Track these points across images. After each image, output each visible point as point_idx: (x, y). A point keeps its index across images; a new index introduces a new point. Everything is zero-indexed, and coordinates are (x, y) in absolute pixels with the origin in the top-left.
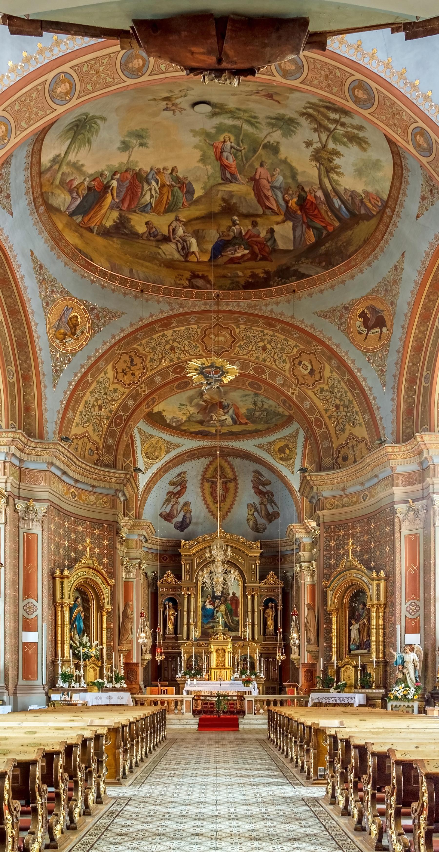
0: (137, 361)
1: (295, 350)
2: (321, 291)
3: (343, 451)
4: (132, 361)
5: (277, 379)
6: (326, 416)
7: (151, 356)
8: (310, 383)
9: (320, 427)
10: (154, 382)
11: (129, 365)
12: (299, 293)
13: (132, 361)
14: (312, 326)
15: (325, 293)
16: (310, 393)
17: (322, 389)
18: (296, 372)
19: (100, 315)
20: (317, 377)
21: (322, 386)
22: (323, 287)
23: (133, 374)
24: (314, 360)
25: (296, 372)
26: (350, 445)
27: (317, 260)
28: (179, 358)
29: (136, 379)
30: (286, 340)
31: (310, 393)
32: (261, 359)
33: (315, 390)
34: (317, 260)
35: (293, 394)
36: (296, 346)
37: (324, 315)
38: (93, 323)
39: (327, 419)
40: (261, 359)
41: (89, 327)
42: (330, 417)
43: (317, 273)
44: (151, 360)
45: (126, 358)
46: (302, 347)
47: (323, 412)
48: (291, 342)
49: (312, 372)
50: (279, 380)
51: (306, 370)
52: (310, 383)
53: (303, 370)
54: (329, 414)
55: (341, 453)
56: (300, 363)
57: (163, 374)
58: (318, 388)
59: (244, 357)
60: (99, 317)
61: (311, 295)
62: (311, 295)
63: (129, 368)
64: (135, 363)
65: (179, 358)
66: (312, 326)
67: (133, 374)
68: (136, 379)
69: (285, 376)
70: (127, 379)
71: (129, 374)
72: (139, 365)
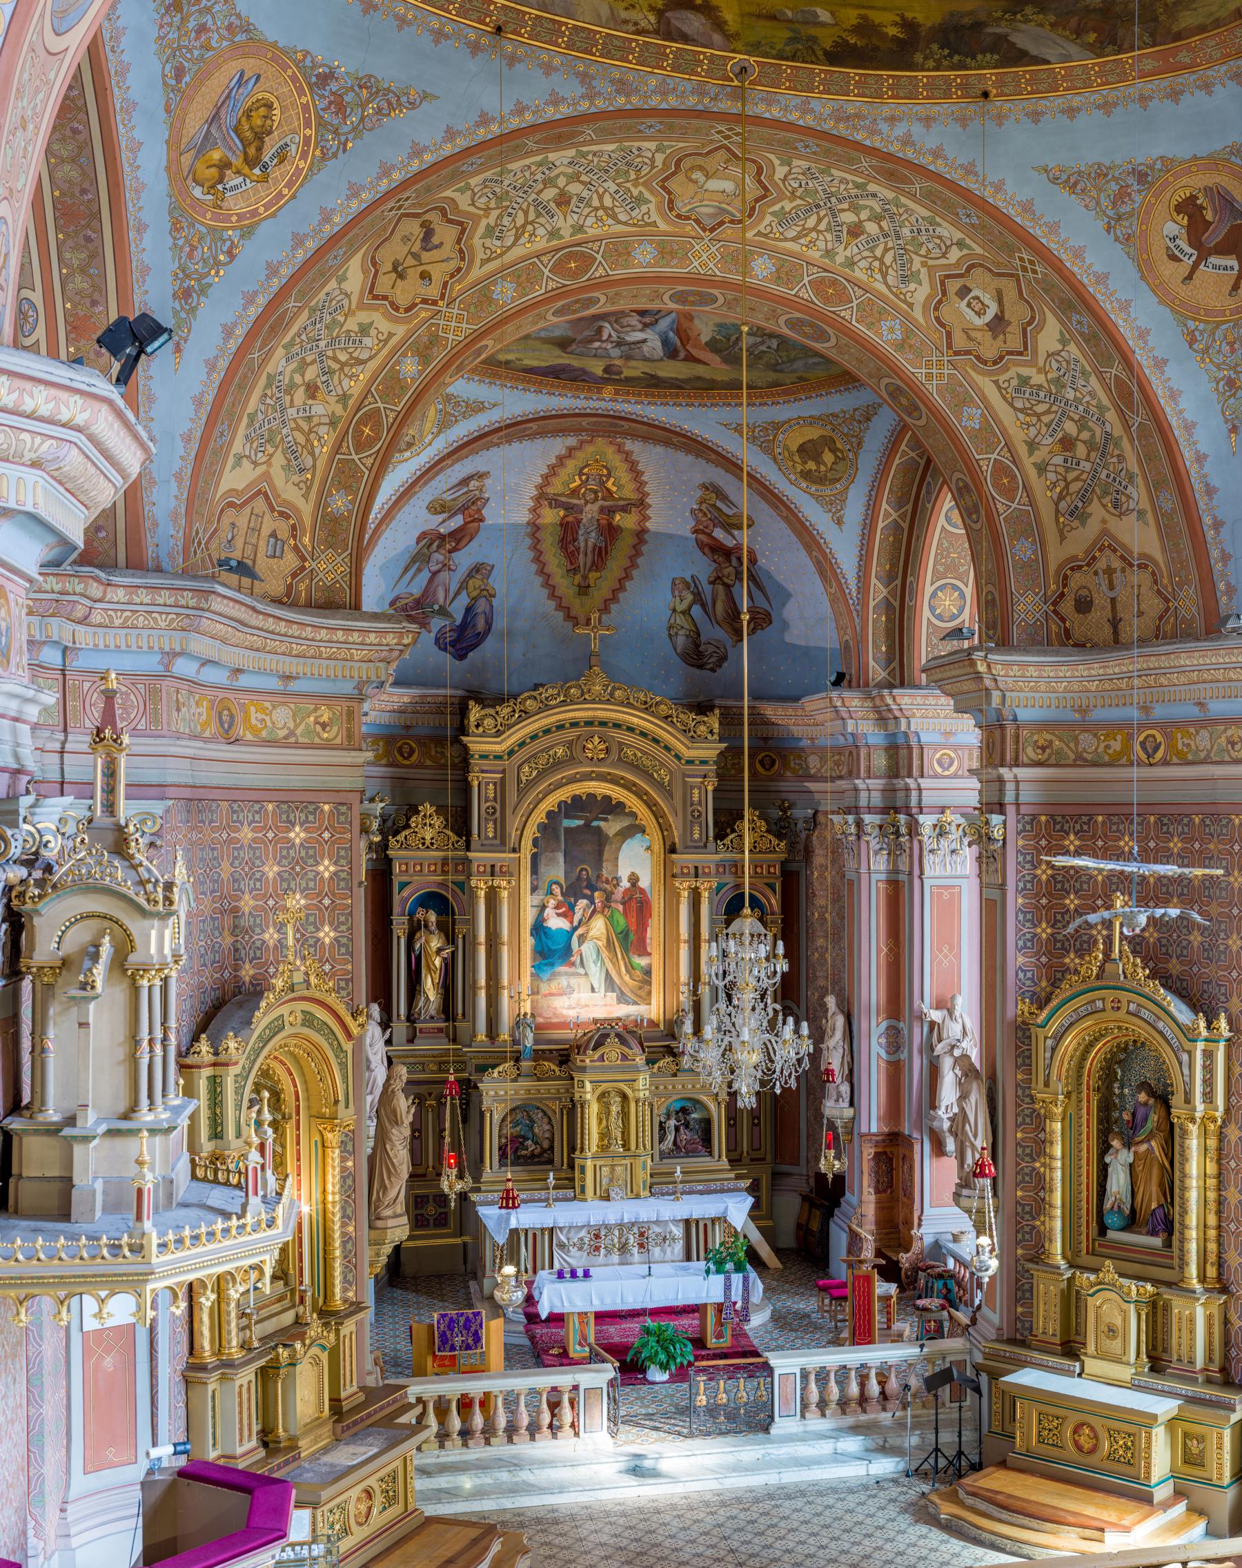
0: (445, 234)
1: (955, 254)
2: (1071, 112)
3: (1077, 580)
4: (428, 233)
5: (885, 325)
6: (1028, 462)
7: (492, 220)
8: (989, 352)
9: (1010, 493)
10: (490, 300)
11: (416, 248)
12: (998, 104)
13: (428, 233)
14: (1027, 207)
15: (1082, 119)
16: (986, 384)
17: (1024, 381)
18: (946, 313)
19: (348, 98)
20: (1014, 342)
21: (1025, 371)
22: (1076, 101)
23: (425, 276)
24: (1010, 295)
25: (946, 313)
26: (1101, 564)
27: (1074, 21)
28: (579, 228)
29: (433, 291)
30: (932, 223)
31: (986, 384)
32: (840, 259)
33: (1002, 378)
34: (1074, 21)
35: (929, 376)
36: (960, 244)
37: (1071, 182)
38: (321, 123)
39: (1032, 473)
40: (840, 259)
41: (307, 140)
42: (1042, 468)
43: (1068, 58)
44: (490, 232)
45: (413, 228)
46: (979, 251)
47: (1022, 450)
48: (947, 231)
49: (998, 324)
50: (891, 330)
51: (978, 314)
52: (989, 352)
53: (970, 314)
54: (1039, 456)
55: (1073, 584)
56: (964, 292)
57: (524, 273)
58: (1012, 373)
59: (789, 245)
60: (345, 104)
61: (1036, 116)
62: (1036, 116)
63: (416, 256)
64: (435, 240)
65: (579, 228)
66: (1027, 207)
67: (425, 276)
68: (433, 291)
69: (913, 321)
70: (404, 293)
71: (413, 274)
72: (448, 250)
